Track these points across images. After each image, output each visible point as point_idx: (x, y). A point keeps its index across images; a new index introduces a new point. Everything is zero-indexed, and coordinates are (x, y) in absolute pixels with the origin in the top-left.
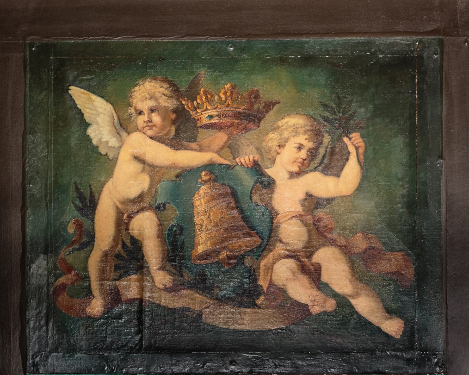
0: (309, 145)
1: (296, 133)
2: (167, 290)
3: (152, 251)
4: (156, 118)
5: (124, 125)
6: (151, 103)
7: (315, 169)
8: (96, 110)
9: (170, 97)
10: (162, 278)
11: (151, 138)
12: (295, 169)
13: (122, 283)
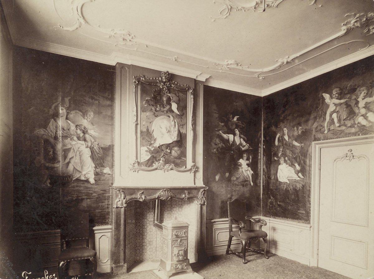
0: (366, 92)
1: (363, 91)
2: (338, 127)
3: (336, 120)
4: (337, 95)
5: (331, 97)
6: (336, 93)
7: (367, 97)
8: (327, 96)
9: (339, 90)
10: (337, 125)
11: (336, 99)
12: (363, 98)
13: (330, 127)
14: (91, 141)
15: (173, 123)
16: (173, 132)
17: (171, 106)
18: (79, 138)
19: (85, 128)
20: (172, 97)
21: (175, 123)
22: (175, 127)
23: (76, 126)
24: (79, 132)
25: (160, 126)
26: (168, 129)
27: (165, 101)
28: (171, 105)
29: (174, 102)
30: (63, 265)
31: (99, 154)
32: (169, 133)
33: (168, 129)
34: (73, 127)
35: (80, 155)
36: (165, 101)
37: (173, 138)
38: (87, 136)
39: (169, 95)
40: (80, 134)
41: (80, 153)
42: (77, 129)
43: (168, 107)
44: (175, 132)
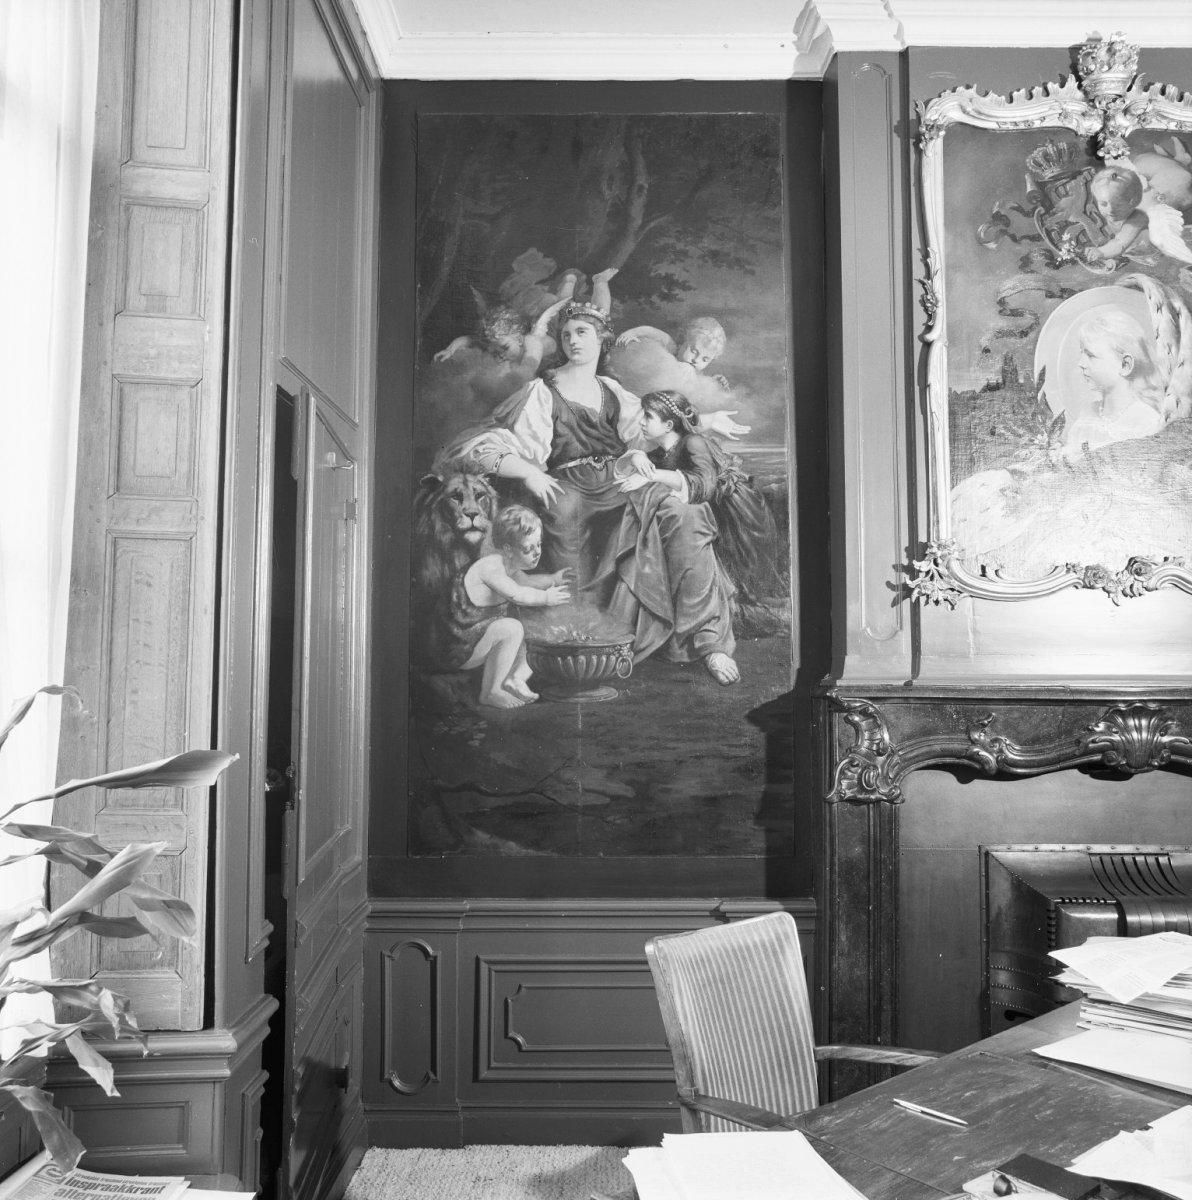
14: (716, 466)
15: (1162, 320)
16: (1164, 370)
17: (1146, 227)
18: (658, 457)
19: (684, 404)
20: (1148, 180)
21: (1175, 315)
22: (1178, 340)
23: (647, 401)
24: (658, 427)
25: (1082, 344)
26: (1135, 351)
27: (1105, 204)
28: (1138, 219)
29: (1163, 198)
30: (557, 662)
31: (755, 528)
32: (1139, 382)
33: (1135, 351)
34: (630, 406)
35: (664, 541)
36: (1105, 204)
37: (1168, 402)
38: (696, 444)
39: (1126, 164)
40: (662, 437)
41: (662, 531)
42: (648, 416)
43: (1124, 234)
44: (1177, 371)
